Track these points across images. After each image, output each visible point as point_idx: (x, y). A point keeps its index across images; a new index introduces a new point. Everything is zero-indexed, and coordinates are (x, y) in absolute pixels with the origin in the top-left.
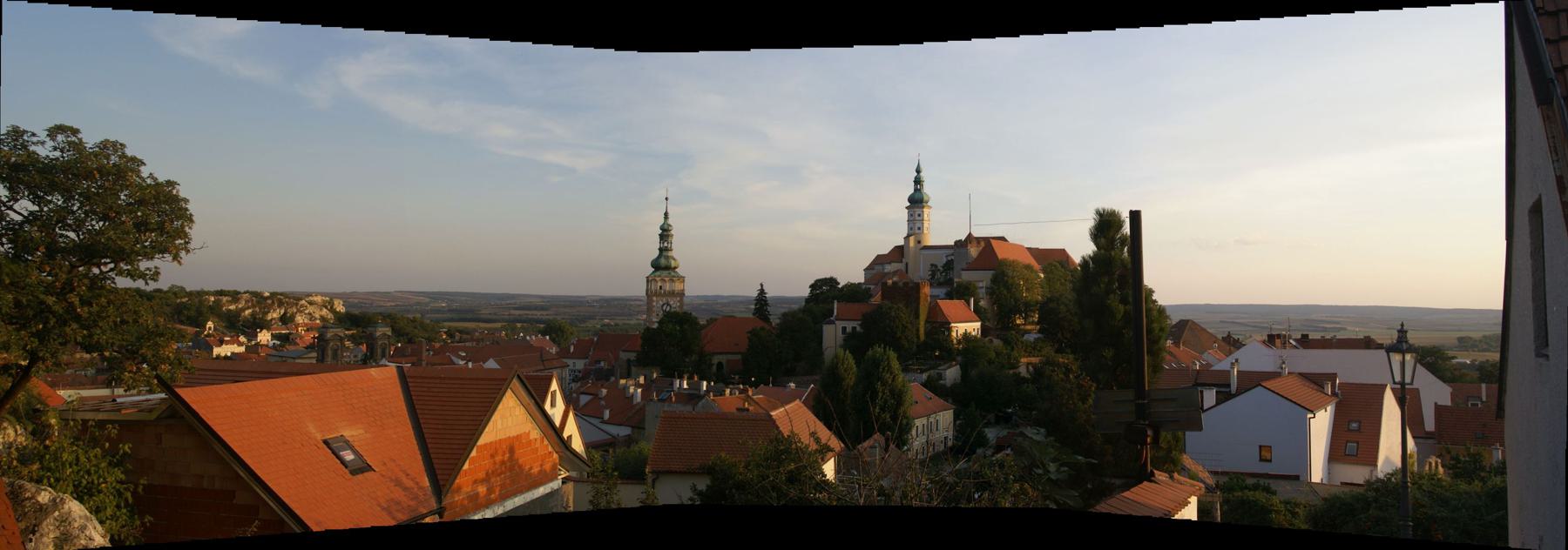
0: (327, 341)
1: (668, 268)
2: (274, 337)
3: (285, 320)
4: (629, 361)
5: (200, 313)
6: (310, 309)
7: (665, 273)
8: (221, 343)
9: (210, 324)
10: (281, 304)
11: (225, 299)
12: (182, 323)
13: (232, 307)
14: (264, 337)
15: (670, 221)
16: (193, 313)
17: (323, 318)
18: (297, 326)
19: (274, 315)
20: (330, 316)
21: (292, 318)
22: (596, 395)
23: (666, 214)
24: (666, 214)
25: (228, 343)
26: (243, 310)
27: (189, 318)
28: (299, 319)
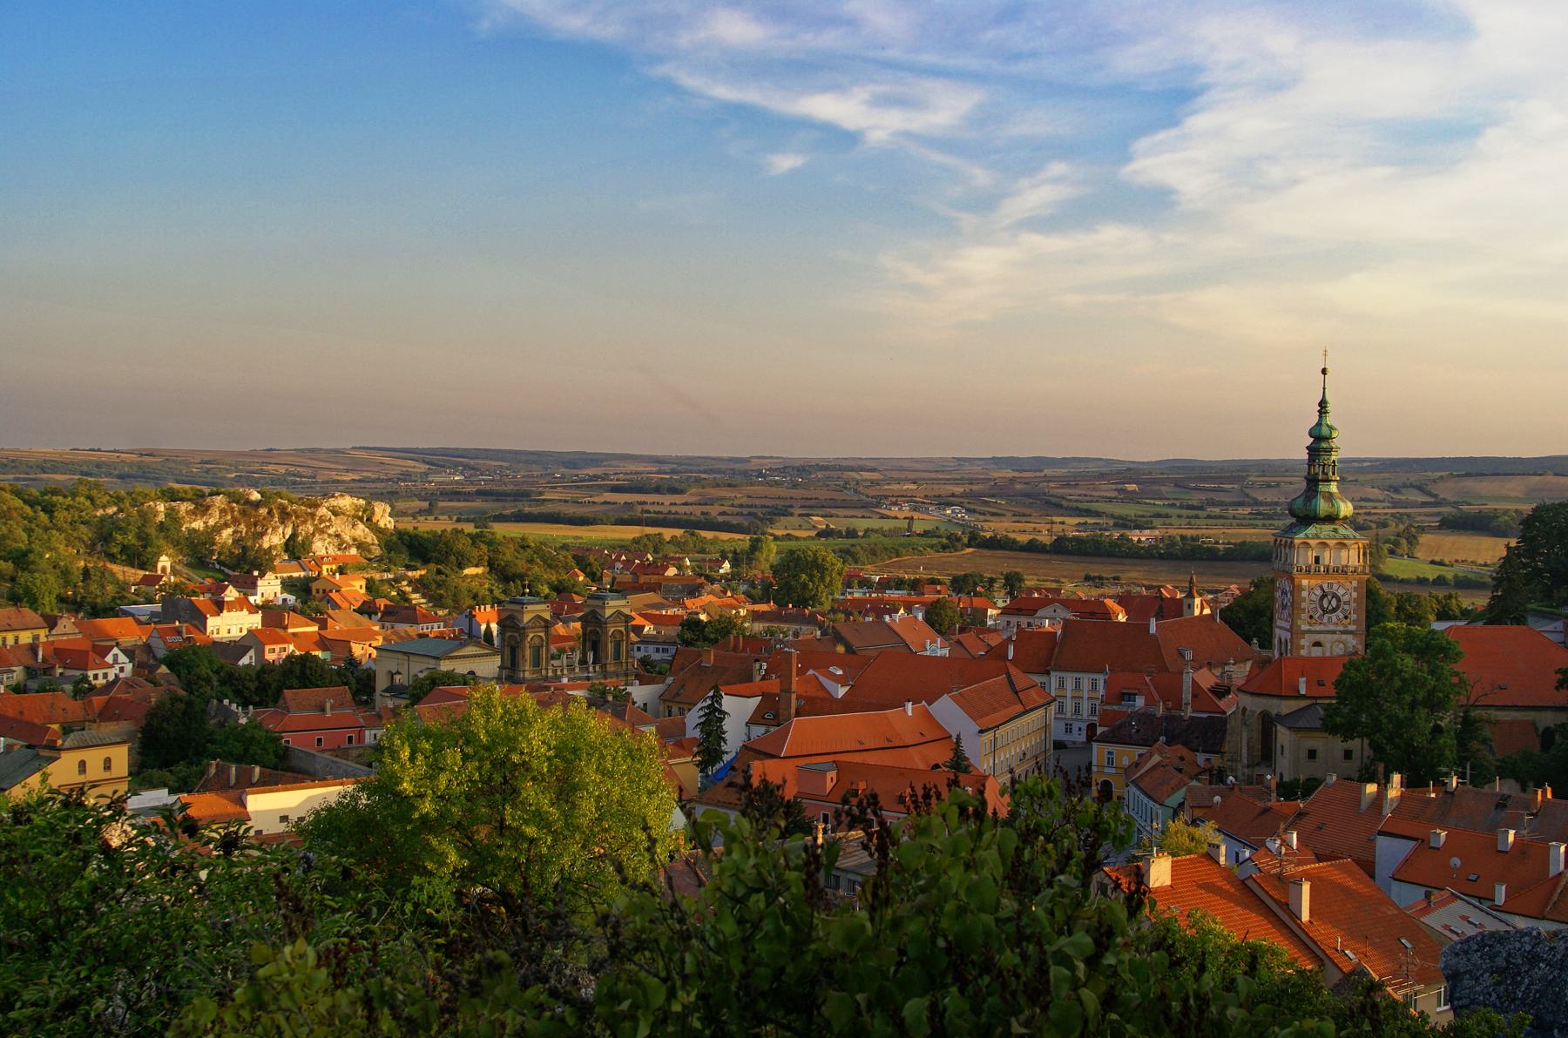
0: (522, 632)
1: (1331, 519)
2: (288, 585)
3: (295, 549)
4: (1268, 723)
5: (145, 540)
6: (338, 526)
7: (1327, 529)
8: (220, 606)
9: (164, 562)
10: (285, 516)
11: (184, 507)
12: (112, 558)
13: (198, 524)
14: (269, 587)
15: (1329, 420)
16: (131, 539)
17: (361, 546)
18: (319, 561)
19: (274, 539)
20: (371, 538)
21: (307, 546)
22: (1423, 842)
23: (1323, 404)
24: (1323, 404)
25: (233, 606)
26: (217, 529)
27: (124, 549)
28: (320, 547)
